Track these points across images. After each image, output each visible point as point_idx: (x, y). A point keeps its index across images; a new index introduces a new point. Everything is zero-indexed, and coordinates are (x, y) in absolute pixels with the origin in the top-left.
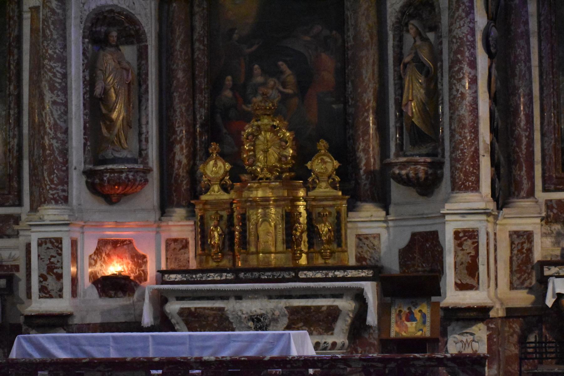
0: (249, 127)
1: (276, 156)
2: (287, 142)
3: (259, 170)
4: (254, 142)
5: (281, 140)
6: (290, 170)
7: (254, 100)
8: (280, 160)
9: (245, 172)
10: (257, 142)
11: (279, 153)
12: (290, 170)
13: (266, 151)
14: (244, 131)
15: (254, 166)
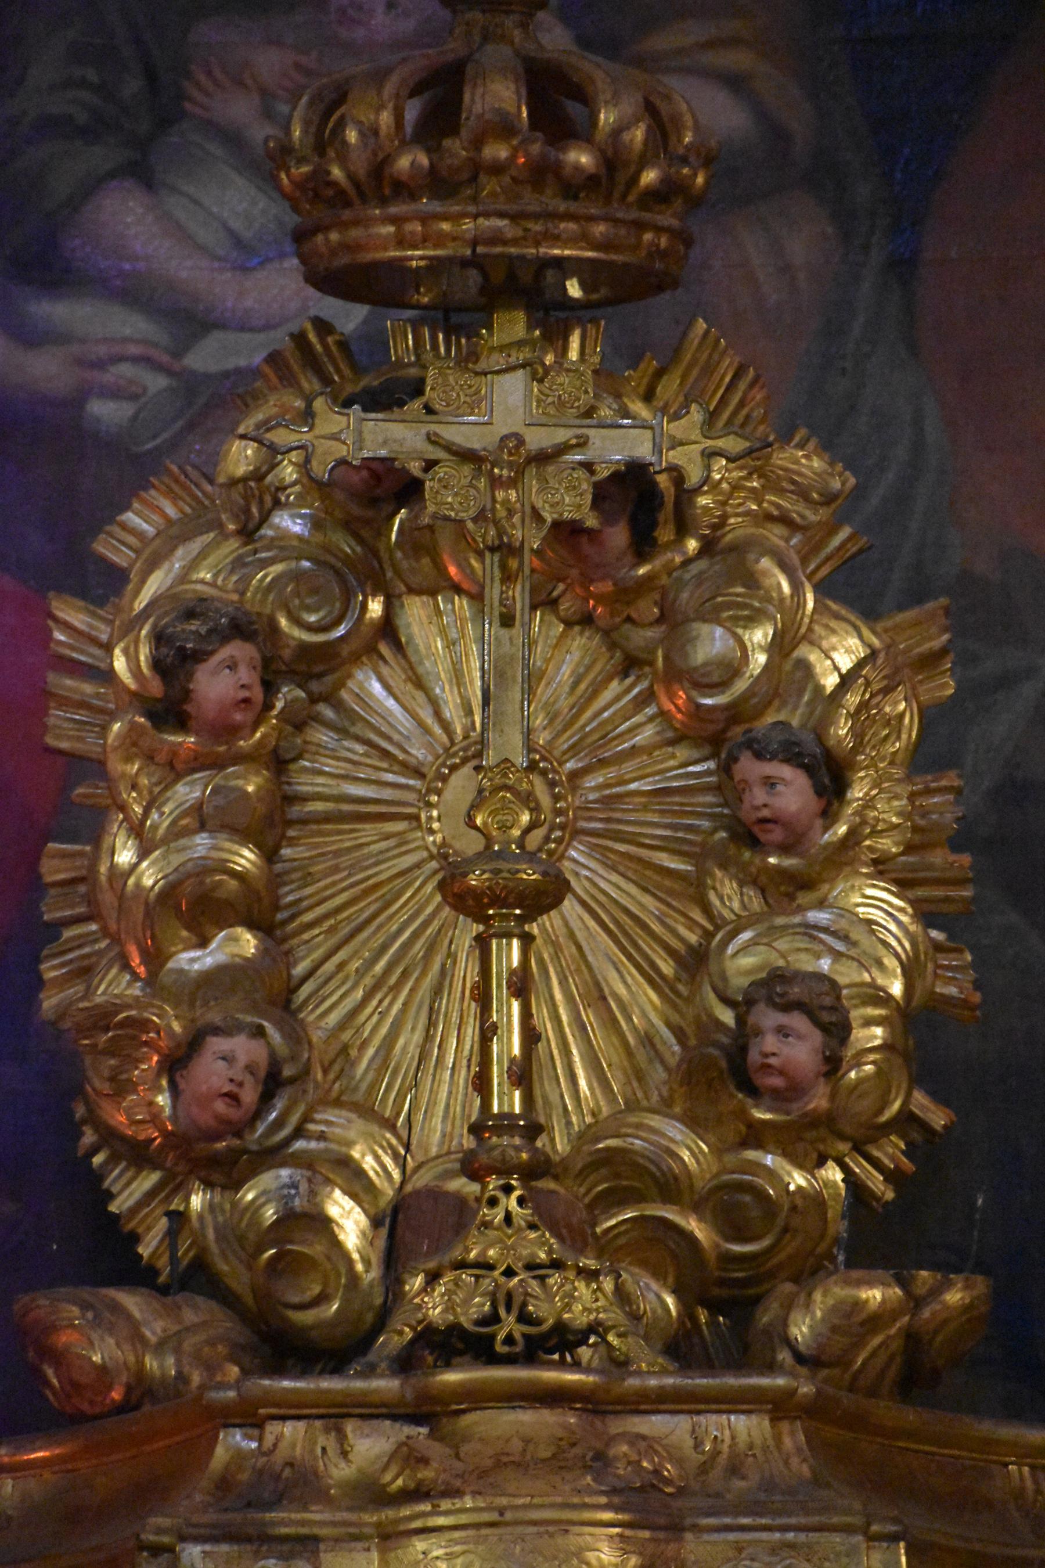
0: (174, 535)
1: (644, 1005)
2: (831, 777)
3: (349, 1220)
4: (278, 762)
5: (723, 735)
6: (875, 1235)
7: (128, 223)
8: (719, 1072)
9: (109, 1256)
10: (328, 772)
11: (696, 961)
12: (875, 1235)
13: (505, 898)
14: (106, 585)
15: (271, 1156)
